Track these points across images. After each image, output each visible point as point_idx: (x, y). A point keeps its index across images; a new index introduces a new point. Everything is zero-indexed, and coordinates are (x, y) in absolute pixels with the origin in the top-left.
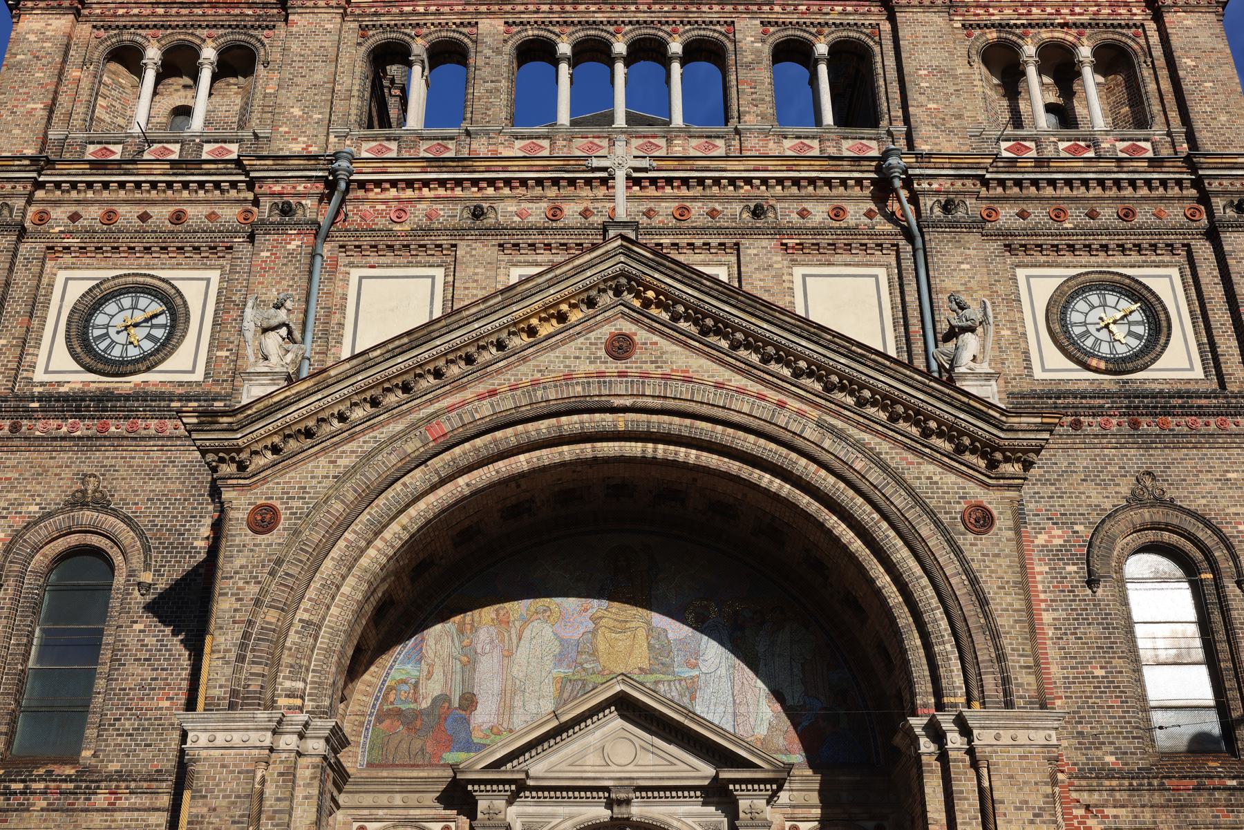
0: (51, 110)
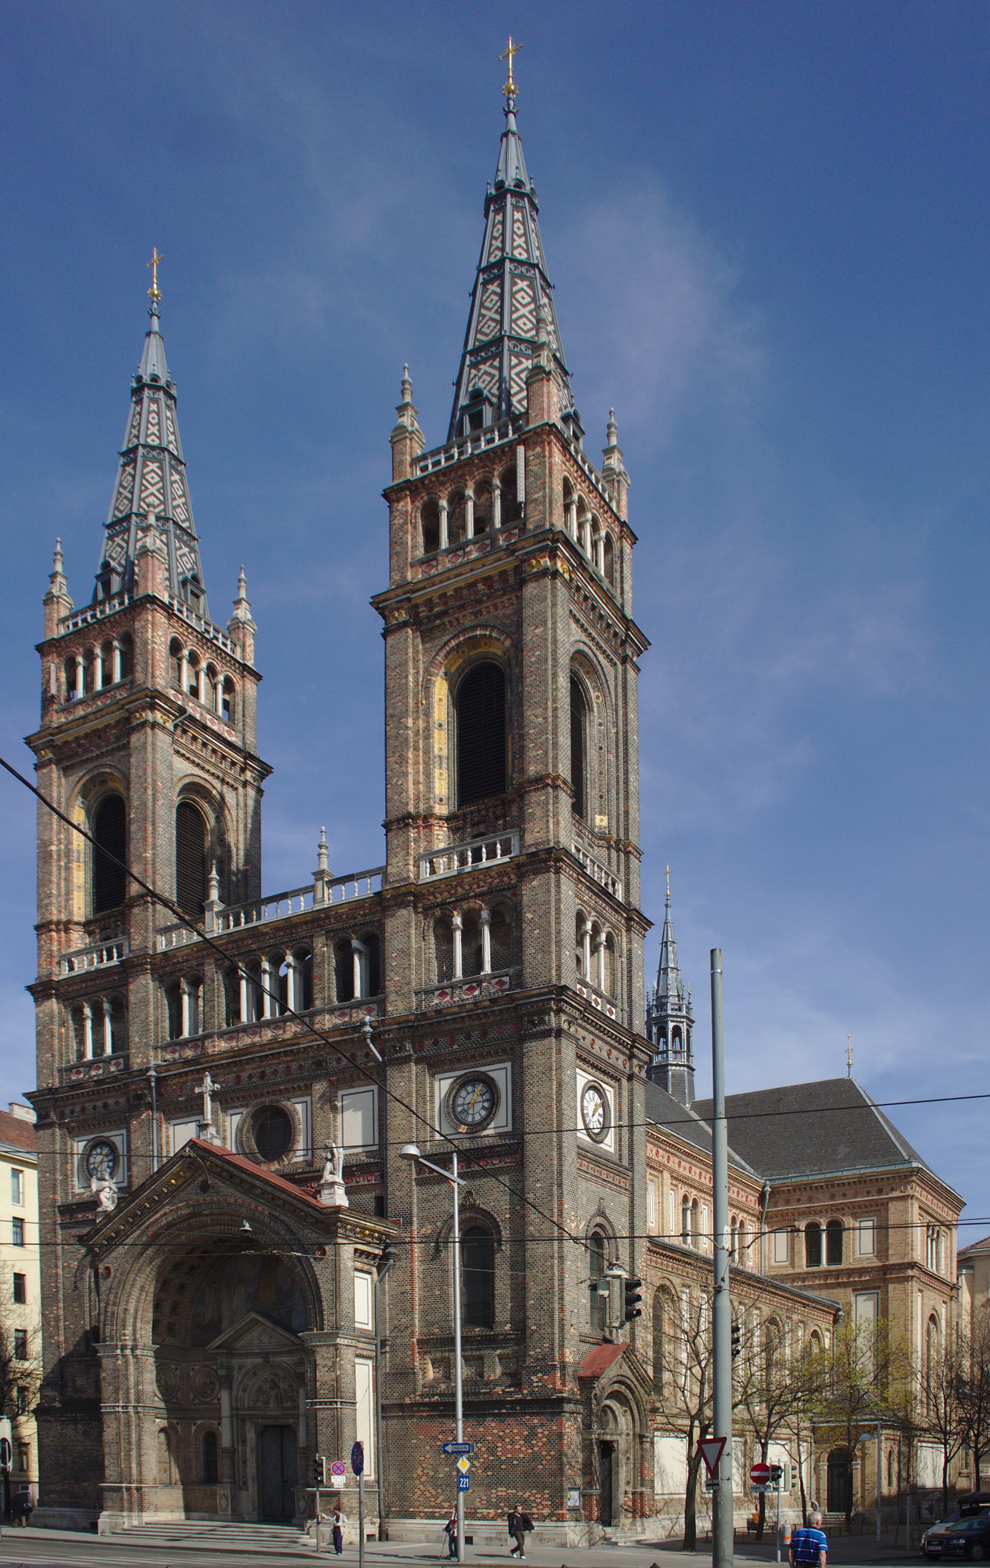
0: (53, 1056)
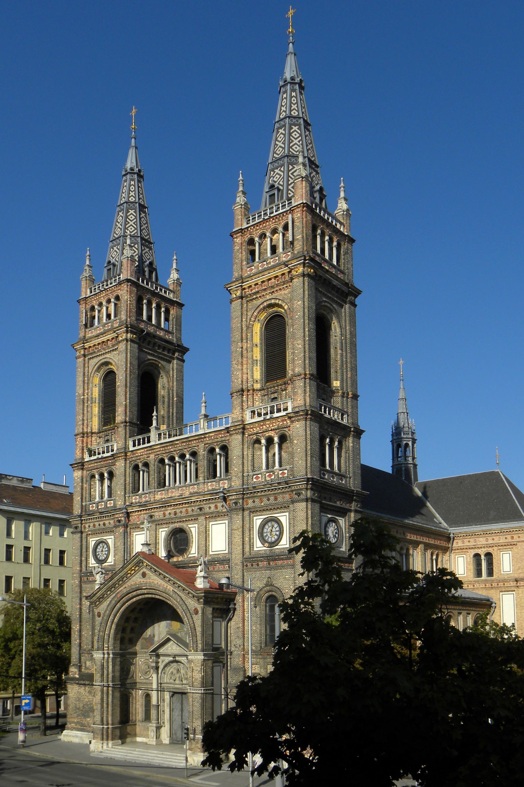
0: (82, 499)
